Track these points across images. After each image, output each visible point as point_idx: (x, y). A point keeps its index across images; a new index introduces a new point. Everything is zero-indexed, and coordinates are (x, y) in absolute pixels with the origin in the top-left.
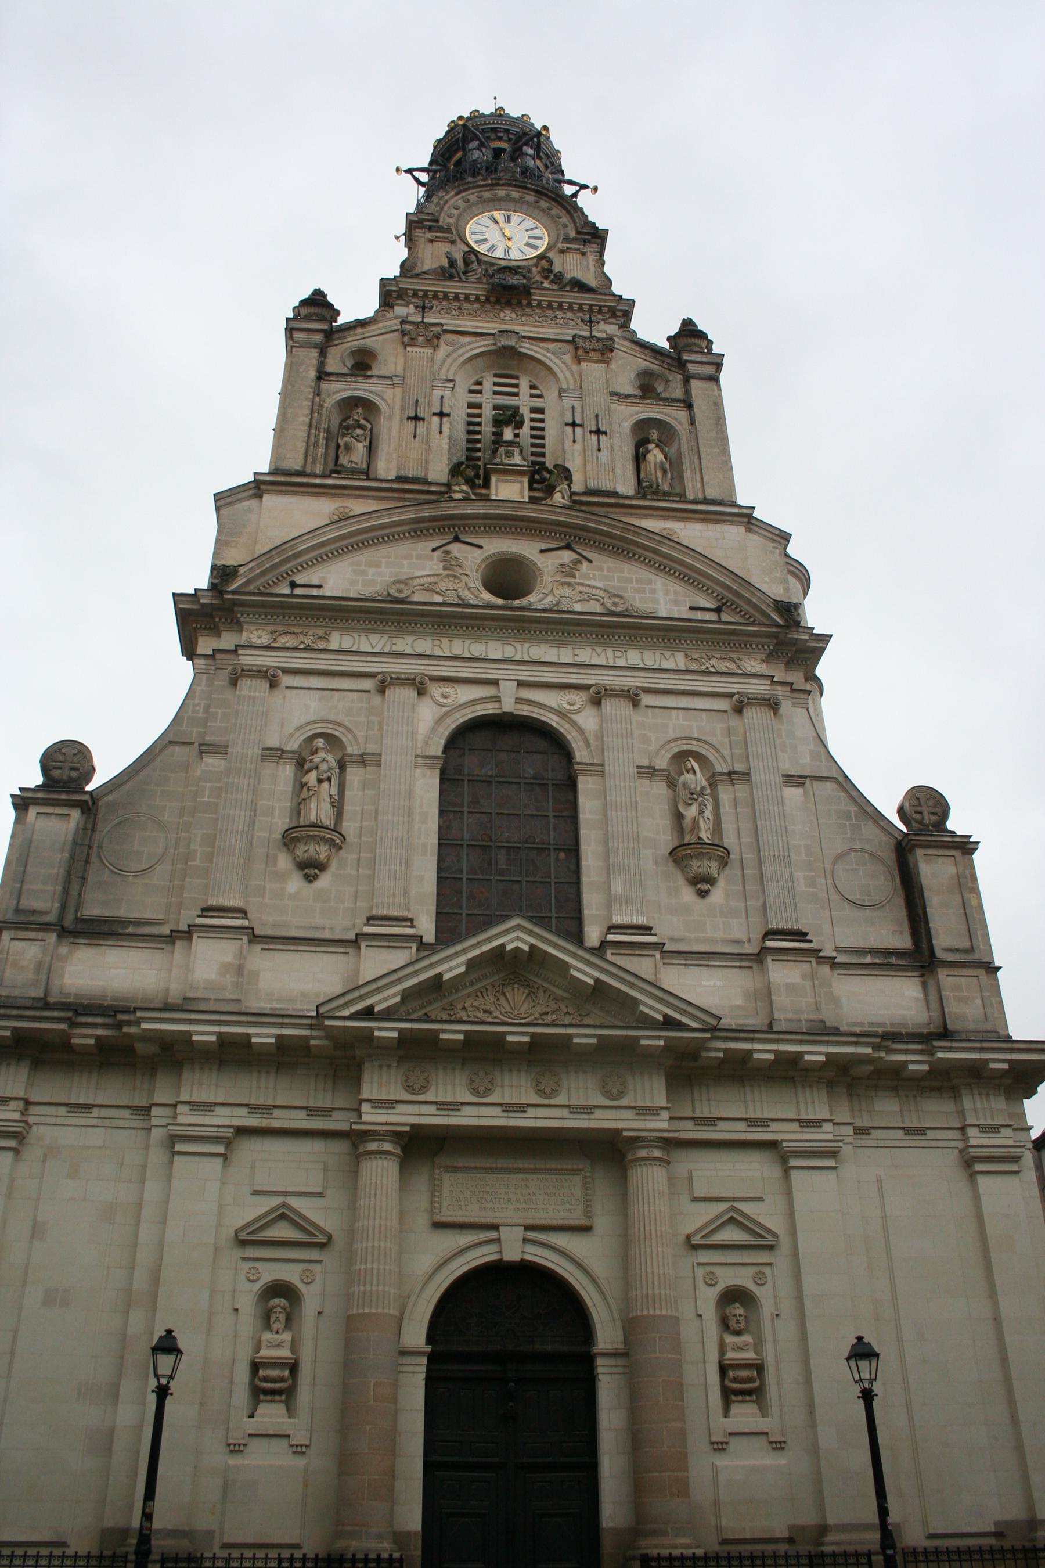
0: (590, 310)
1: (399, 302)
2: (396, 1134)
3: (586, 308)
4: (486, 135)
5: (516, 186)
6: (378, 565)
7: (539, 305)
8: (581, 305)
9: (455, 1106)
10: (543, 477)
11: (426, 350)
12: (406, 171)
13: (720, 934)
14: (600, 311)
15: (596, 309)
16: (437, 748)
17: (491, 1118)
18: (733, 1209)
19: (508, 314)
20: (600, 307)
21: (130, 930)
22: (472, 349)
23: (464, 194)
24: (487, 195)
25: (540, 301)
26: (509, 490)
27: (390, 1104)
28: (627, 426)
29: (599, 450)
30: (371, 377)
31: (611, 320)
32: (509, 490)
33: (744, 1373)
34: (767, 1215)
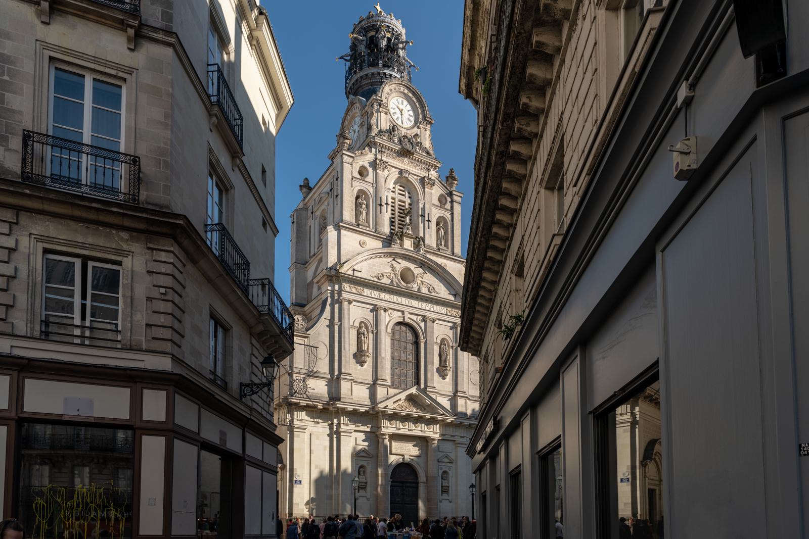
2: (389, 434)
6: (374, 265)
7: (415, 160)
9: (400, 429)
10: (419, 242)
13: (448, 390)
16: (389, 330)
17: (406, 432)
18: (447, 455)
21: (322, 376)
26: (408, 244)
27: (387, 428)
28: (436, 217)
30: (366, 181)
32: (408, 244)
33: (446, 488)
34: (452, 456)
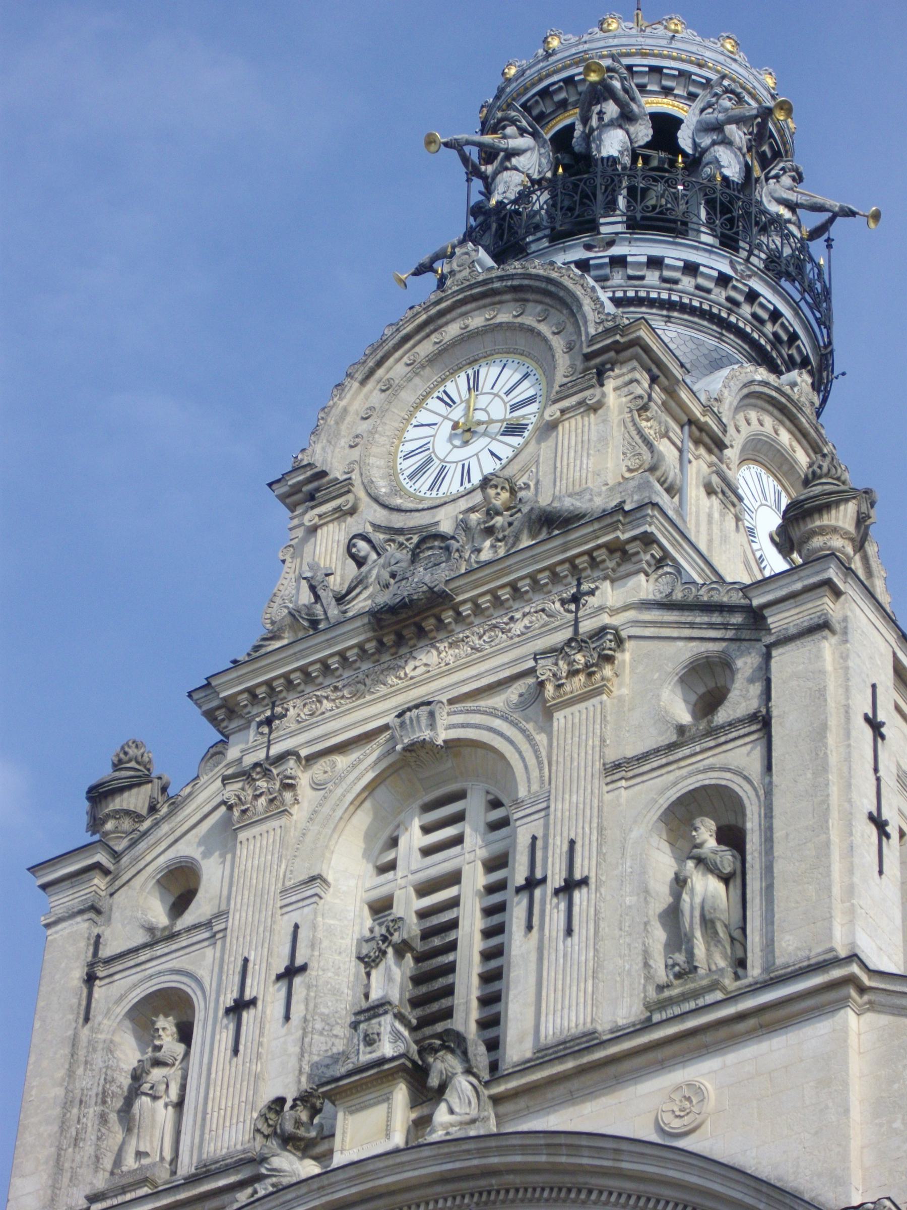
1: (233, 725)
3: (563, 570)
4: (535, 112)
5: (474, 298)
7: (478, 610)
11: (275, 823)
12: (418, 272)
14: (594, 563)
15: (582, 562)
20: (589, 553)
22: (358, 779)
23: (380, 372)
24: (426, 348)
25: (474, 601)
29: (569, 932)
31: (624, 569)
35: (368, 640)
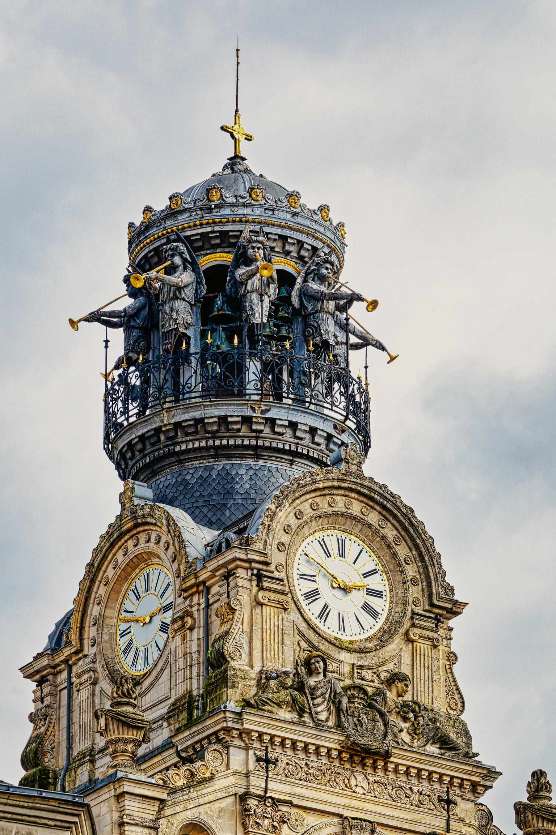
0: (451, 783)
1: (237, 742)
3: (446, 779)
7: (396, 771)
8: (441, 775)
14: (461, 786)
15: (457, 781)
19: (359, 780)
20: (462, 780)
23: (298, 501)
24: (323, 504)
35: (335, 749)
